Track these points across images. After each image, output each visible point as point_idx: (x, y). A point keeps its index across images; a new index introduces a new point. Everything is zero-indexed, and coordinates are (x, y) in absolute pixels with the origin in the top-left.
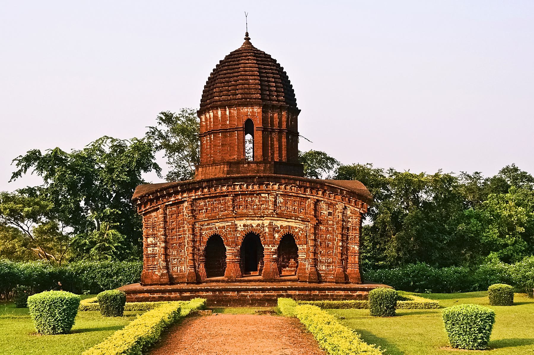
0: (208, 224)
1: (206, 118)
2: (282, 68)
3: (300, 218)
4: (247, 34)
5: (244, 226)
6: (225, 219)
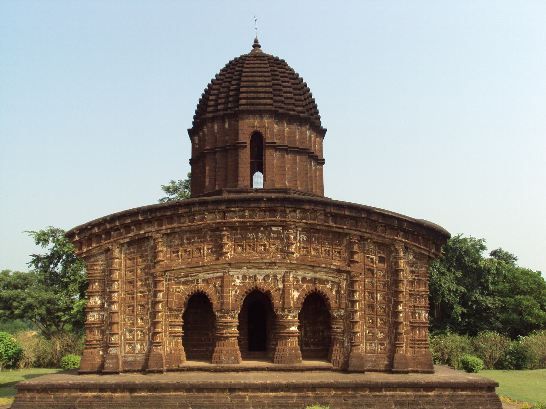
1: (199, 137)
3: (335, 265)
4: (256, 41)
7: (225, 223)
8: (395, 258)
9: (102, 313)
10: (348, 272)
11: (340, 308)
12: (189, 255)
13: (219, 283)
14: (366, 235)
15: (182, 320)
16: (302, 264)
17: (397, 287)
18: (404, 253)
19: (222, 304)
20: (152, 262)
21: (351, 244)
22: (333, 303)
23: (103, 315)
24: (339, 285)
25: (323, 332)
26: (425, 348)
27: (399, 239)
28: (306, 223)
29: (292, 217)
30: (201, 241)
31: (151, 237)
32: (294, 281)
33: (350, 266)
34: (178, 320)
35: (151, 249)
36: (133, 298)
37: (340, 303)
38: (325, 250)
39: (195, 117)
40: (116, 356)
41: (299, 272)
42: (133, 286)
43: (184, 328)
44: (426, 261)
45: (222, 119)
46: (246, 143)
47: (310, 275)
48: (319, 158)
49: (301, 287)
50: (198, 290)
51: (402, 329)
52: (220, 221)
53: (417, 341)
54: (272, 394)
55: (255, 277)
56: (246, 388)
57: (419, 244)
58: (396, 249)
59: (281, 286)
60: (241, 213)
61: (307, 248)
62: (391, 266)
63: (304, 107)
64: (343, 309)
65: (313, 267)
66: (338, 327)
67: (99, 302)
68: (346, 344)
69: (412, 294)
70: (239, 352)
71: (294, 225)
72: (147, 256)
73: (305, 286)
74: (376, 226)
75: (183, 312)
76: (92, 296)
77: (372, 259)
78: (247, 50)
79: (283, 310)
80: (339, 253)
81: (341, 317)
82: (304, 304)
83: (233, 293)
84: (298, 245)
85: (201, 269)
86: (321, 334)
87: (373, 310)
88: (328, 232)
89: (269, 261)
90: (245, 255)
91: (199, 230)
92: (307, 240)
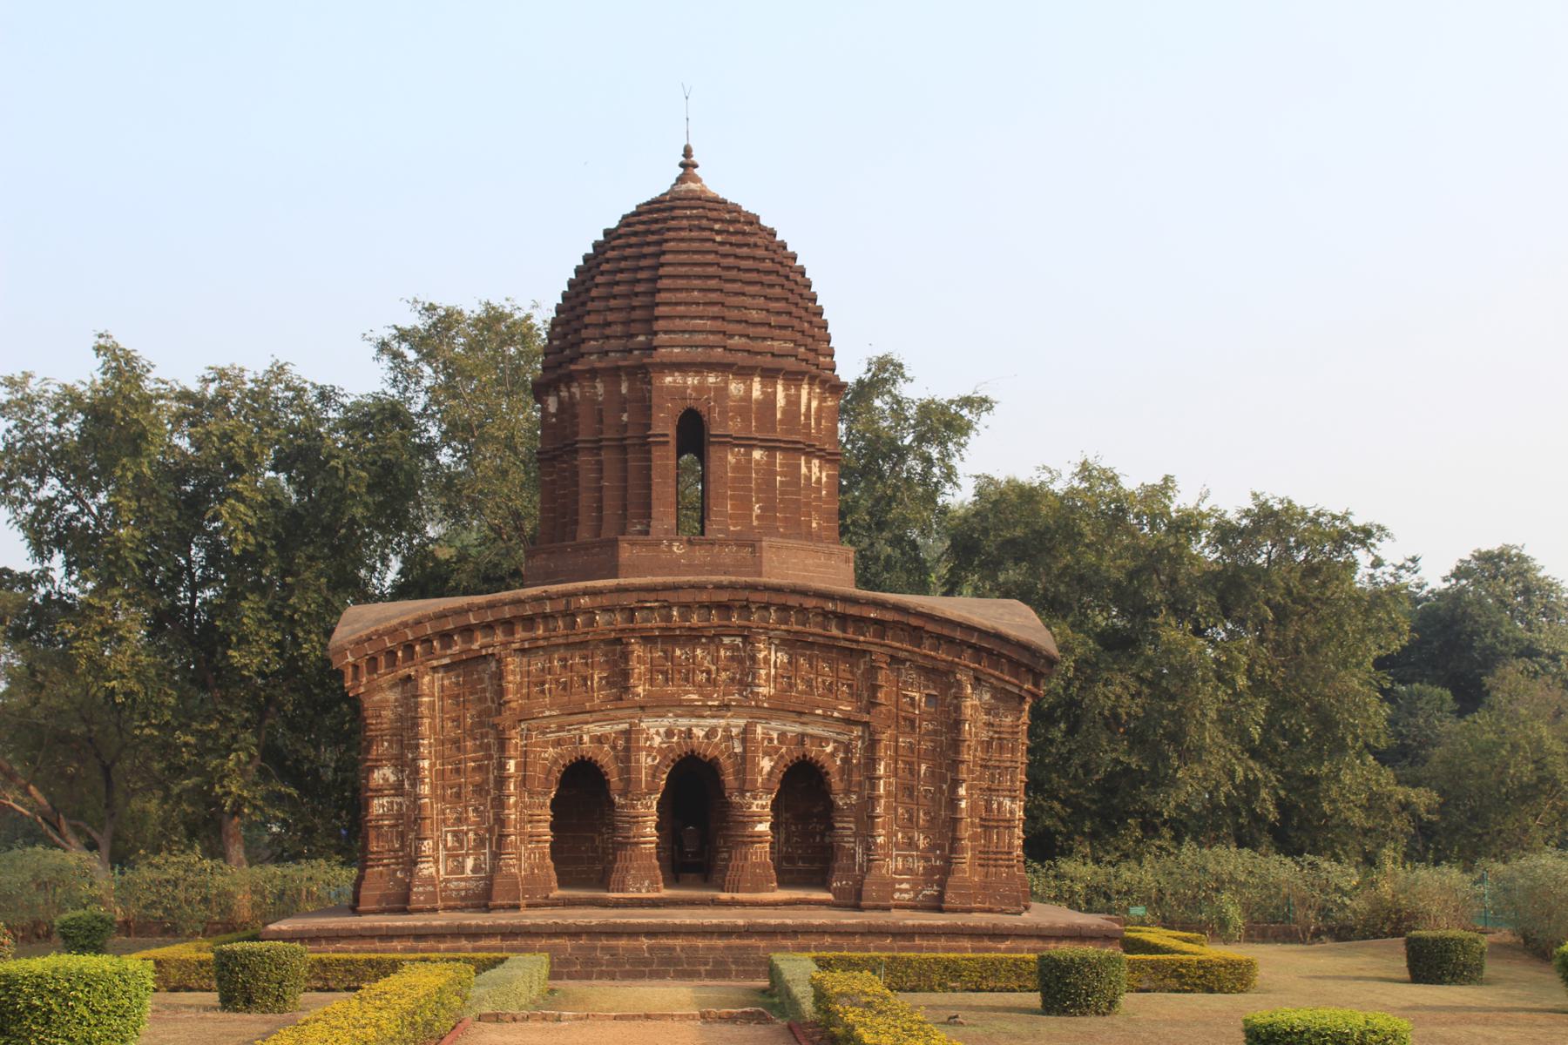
0: (561, 728)
1: (560, 402)
2: (794, 257)
4: (687, 152)
5: (669, 733)
6: (612, 714)
7: (633, 630)
9: (399, 800)
10: (866, 724)
11: (847, 792)
12: (564, 689)
13: (621, 743)
16: (779, 708)
17: (957, 752)
18: (974, 689)
19: (628, 781)
21: (873, 670)
22: (835, 781)
23: (400, 804)
24: (847, 748)
28: (788, 631)
40: (431, 880)
41: (773, 724)
42: (458, 749)
43: (553, 827)
44: (1015, 704)
47: (794, 729)
51: (965, 833)
54: (721, 943)
55: (689, 733)
60: (664, 612)
65: (801, 714)
66: (846, 827)
67: (392, 778)
68: (858, 858)
69: (986, 767)
70: (659, 872)
72: (484, 690)
77: (913, 699)
79: (742, 792)
80: (850, 686)
82: (783, 782)
87: (911, 796)
88: (830, 648)
90: (670, 689)
91: (583, 644)
92: (790, 662)
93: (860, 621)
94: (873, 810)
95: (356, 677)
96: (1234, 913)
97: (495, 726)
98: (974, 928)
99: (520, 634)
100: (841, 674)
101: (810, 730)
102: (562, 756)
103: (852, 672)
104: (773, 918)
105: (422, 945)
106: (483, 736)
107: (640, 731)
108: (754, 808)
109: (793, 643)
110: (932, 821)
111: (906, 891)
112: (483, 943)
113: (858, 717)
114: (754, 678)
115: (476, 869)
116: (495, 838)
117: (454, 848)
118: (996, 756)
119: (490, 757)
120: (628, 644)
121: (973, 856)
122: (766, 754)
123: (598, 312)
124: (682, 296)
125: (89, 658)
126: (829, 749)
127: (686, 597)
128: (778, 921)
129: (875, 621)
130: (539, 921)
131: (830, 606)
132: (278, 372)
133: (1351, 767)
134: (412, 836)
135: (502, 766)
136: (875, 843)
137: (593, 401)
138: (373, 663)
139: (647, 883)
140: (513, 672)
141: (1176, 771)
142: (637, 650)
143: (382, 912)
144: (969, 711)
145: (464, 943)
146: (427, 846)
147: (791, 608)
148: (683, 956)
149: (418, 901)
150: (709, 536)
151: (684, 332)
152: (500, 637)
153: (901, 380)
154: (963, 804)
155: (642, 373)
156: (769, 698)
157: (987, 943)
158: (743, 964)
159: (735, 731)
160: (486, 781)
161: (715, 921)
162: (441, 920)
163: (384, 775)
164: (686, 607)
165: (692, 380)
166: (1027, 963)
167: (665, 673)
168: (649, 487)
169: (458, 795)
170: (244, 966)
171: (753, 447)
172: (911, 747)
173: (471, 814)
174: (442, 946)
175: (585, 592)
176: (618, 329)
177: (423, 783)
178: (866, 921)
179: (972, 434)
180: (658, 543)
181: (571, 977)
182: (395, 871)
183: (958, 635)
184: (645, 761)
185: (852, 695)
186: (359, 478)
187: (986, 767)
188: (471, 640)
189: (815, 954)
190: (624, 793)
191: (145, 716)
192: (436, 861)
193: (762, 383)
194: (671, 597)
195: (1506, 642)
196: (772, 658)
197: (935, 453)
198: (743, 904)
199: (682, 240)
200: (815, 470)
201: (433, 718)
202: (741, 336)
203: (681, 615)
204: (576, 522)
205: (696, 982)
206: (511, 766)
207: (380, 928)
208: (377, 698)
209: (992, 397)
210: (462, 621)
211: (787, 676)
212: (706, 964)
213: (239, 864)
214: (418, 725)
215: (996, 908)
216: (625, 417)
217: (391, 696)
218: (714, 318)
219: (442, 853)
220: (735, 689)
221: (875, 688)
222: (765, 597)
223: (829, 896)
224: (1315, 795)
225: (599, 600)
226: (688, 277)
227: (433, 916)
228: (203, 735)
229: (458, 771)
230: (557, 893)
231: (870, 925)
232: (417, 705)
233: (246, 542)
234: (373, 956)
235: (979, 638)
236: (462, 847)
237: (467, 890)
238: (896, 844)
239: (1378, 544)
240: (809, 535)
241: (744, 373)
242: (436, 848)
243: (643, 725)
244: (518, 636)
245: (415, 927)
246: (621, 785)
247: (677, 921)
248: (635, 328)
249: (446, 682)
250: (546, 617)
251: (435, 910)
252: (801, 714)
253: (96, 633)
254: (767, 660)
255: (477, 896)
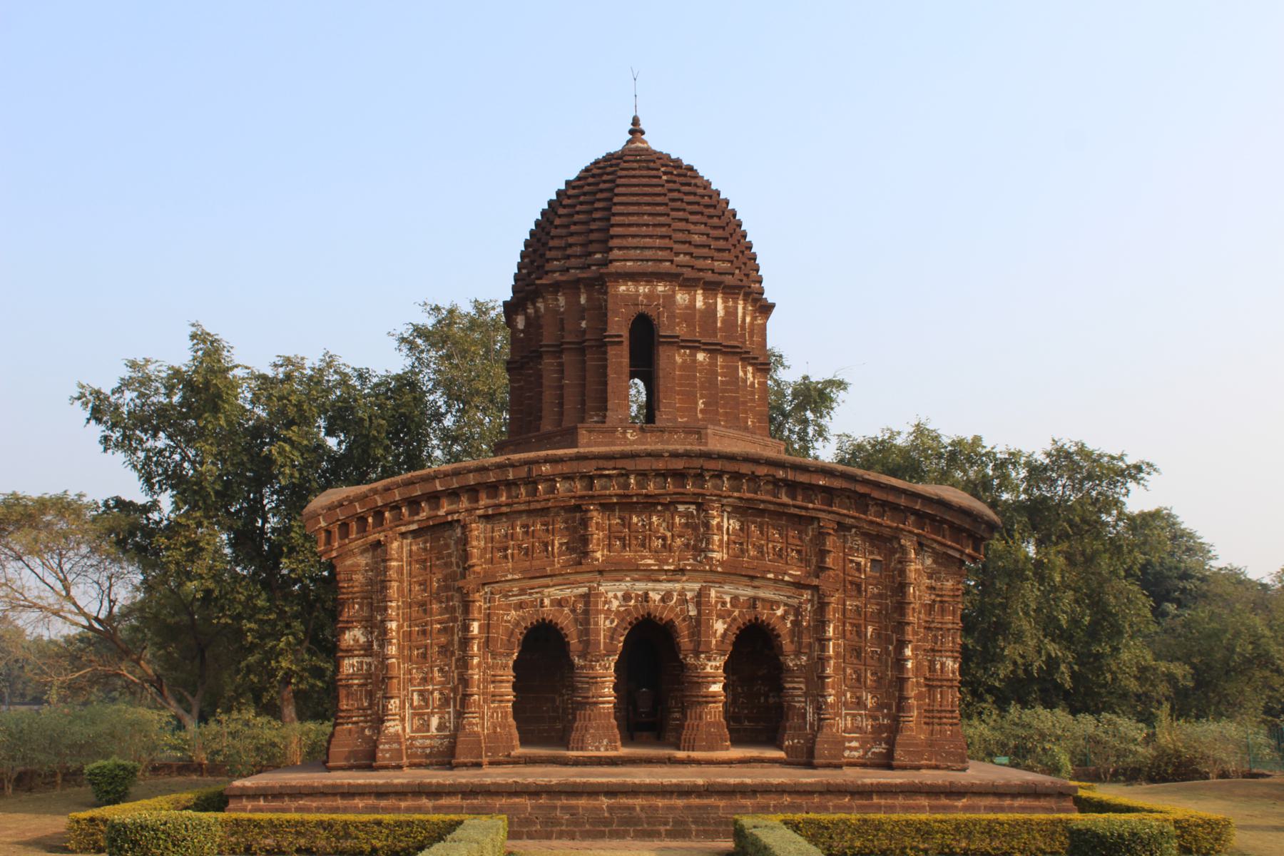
0: (523, 591)
1: (528, 318)
3: (790, 575)
4: (636, 121)
5: (627, 597)
6: (572, 578)
7: (592, 497)
8: (900, 562)
10: (816, 588)
11: (798, 654)
12: (526, 554)
13: (580, 606)
14: (849, 521)
15: (512, 672)
16: (732, 572)
17: (903, 614)
18: (917, 554)
19: (587, 644)
20: (458, 566)
21: (821, 536)
23: (369, 664)
24: (797, 611)
25: (767, 697)
26: (951, 725)
27: (907, 528)
28: (740, 499)
29: (715, 487)
30: (547, 530)
31: (458, 521)
32: (717, 602)
33: (818, 577)
34: (506, 672)
35: (456, 543)
36: (424, 632)
37: (800, 644)
38: (774, 548)
39: (517, 278)
40: (396, 738)
41: (727, 588)
42: (425, 611)
43: (515, 688)
44: (955, 568)
45: (574, 286)
46: (620, 336)
47: (746, 592)
48: (761, 360)
49: (730, 615)
50: (544, 619)
51: (911, 692)
52: (584, 493)
53: (939, 712)
54: (680, 802)
56: (634, 791)
57: (944, 537)
58: (902, 546)
59: (693, 613)
60: (622, 480)
61: (741, 544)
62: (893, 576)
63: (726, 239)
64: (805, 654)
65: (752, 578)
66: (796, 687)
67: (362, 640)
68: (809, 717)
70: (616, 731)
71: (719, 501)
72: (450, 555)
73: (736, 613)
74: (867, 506)
75: (515, 656)
76: (348, 628)
77: (858, 564)
78: (616, 141)
79: (697, 654)
80: (799, 552)
81: (800, 667)
82: (735, 644)
83: (607, 622)
84: (725, 538)
85: (547, 581)
86: (762, 700)
87: (858, 657)
89: (672, 568)
90: (628, 554)
91: (544, 511)
92: (741, 529)
93: (810, 489)
94: (823, 671)
95: (329, 541)
96: (1064, 759)
97: (460, 589)
98: (931, 786)
99: (484, 501)
100: (790, 540)
101: (761, 594)
102: (524, 619)
103: (801, 539)
104: (732, 777)
105: (383, 803)
106: (449, 599)
107: (599, 595)
108: (708, 669)
109: (744, 511)
110: (879, 680)
111: (855, 749)
112: (444, 801)
113: (808, 581)
114: (708, 544)
115: (439, 728)
116: (459, 697)
117: (420, 707)
118: (938, 618)
119: (455, 620)
120: (588, 511)
121: (919, 714)
122: (720, 616)
123: (560, 237)
124: (634, 219)
125: (177, 564)
126: (779, 612)
127: (643, 465)
128: (738, 780)
129: (824, 489)
130: (499, 780)
131: (781, 474)
132: (330, 362)
133: (1126, 646)
134: (379, 694)
135: (466, 628)
136: (826, 703)
137: (557, 312)
138: (345, 527)
139: (605, 742)
140: (478, 538)
141: (1003, 650)
142: (596, 517)
143: (350, 768)
144: (913, 575)
145: (425, 802)
146: (394, 704)
147: (744, 475)
148: (643, 815)
149: (384, 758)
150: (658, 424)
151: (636, 248)
152: (465, 503)
153: (781, 368)
154: (909, 665)
155: (599, 284)
156: (722, 563)
157: (944, 801)
158: (704, 823)
159: (689, 595)
160: (451, 643)
161: (674, 781)
162: (400, 778)
163: (354, 636)
164: (643, 475)
165: (643, 289)
166: (1002, 824)
167: (622, 539)
168: (605, 384)
169: (424, 656)
170: (135, 843)
171: (697, 349)
172: (858, 610)
173: (436, 674)
174: (403, 804)
175: (547, 460)
176: (578, 250)
177: (390, 643)
178: (824, 780)
179: (834, 405)
180: (614, 430)
181: (531, 836)
182: (363, 729)
183: (902, 501)
184: (604, 624)
185: (801, 560)
186: (379, 425)
187: (928, 629)
188: (438, 507)
189: (781, 817)
190: (583, 655)
191: (222, 609)
192: (403, 720)
193: (704, 294)
194: (629, 465)
195: (1170, 569)
196: (725, 524)
197: (809, 415)
198: (698, 762)
199: (634, 177)
200: (750, 376)
201: (401, 581)
202: (685, 254)
203: (637, 483)
204: (540, 418)
205: (657, 843)
206: (475, 628)
207: (342, 786)
208: (348, 562)
209: (846, 380)
210: (428, 488)
211: (739, 542)
212: (666, 824)
213: (292, 721)
214: (386, 588)
215: (942, 765)
216: (584, 324)
217: (363, 560)
218: (662, 237)
219: (408, 712)
220: (689, 554)
221: (823, 553)
222: (719, 465)
223: (782, 754)
224: (1100, 668)
225: (560, 468)
226: (638, 204)
227: (398, 773)
228: (261, 622)
229: (424, 632)
230: (519, 751)
231: (829, 784)
232: (386, 569)
233: (292, 476)
234: (326, 817)
235: (923, 505)
236: (427, 706)
237: (432, 747)
238: (845, 704)
239: (1147, 477)
240: (746, 429)
241: (689, 285)
242: (402, 707)
243: (602, 589)
244: (482, 503)
245: (377, 785)
246: (581, 647)
247: (637, 781)
248: (591, 248)
249: (414, 548)
250: (510, 484)
251: (400, 767)
252: (752, 578)
253: (183, 545)
254: (720, 527)
255: (440, 753)
